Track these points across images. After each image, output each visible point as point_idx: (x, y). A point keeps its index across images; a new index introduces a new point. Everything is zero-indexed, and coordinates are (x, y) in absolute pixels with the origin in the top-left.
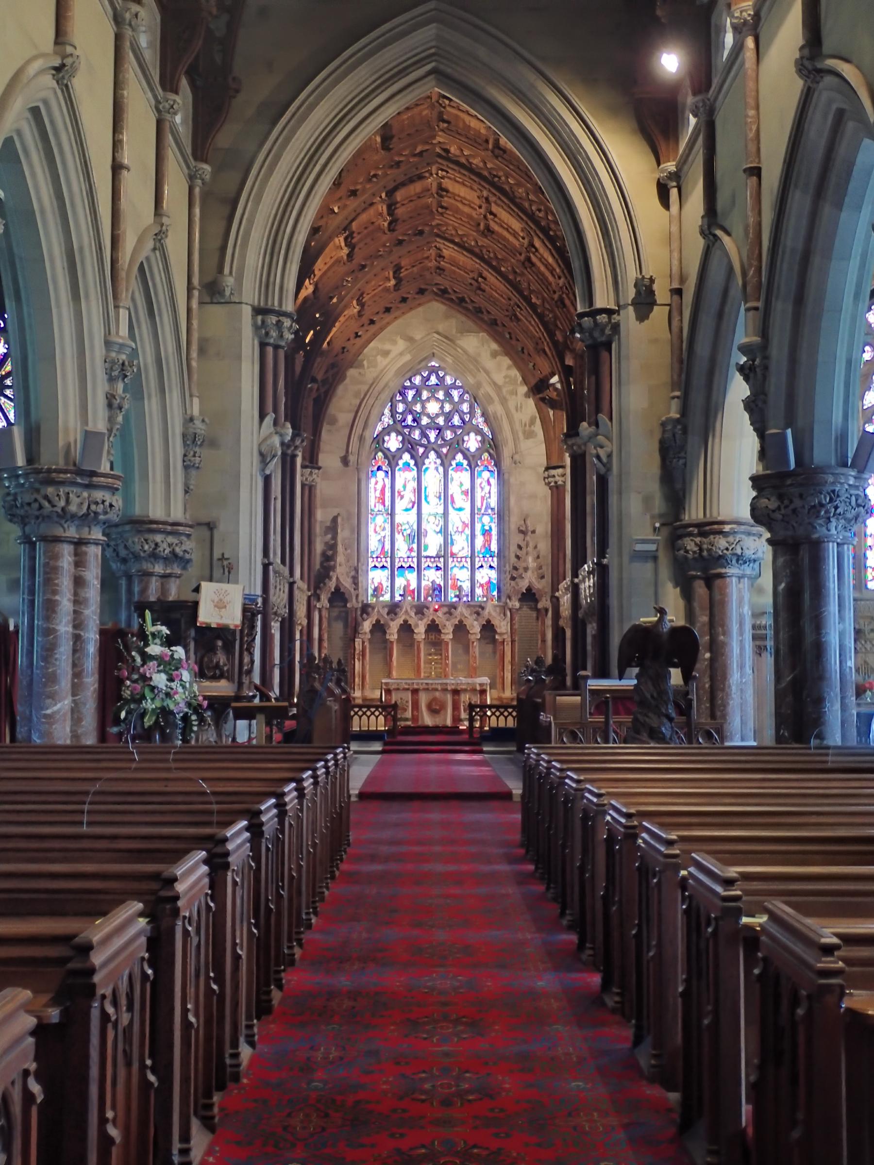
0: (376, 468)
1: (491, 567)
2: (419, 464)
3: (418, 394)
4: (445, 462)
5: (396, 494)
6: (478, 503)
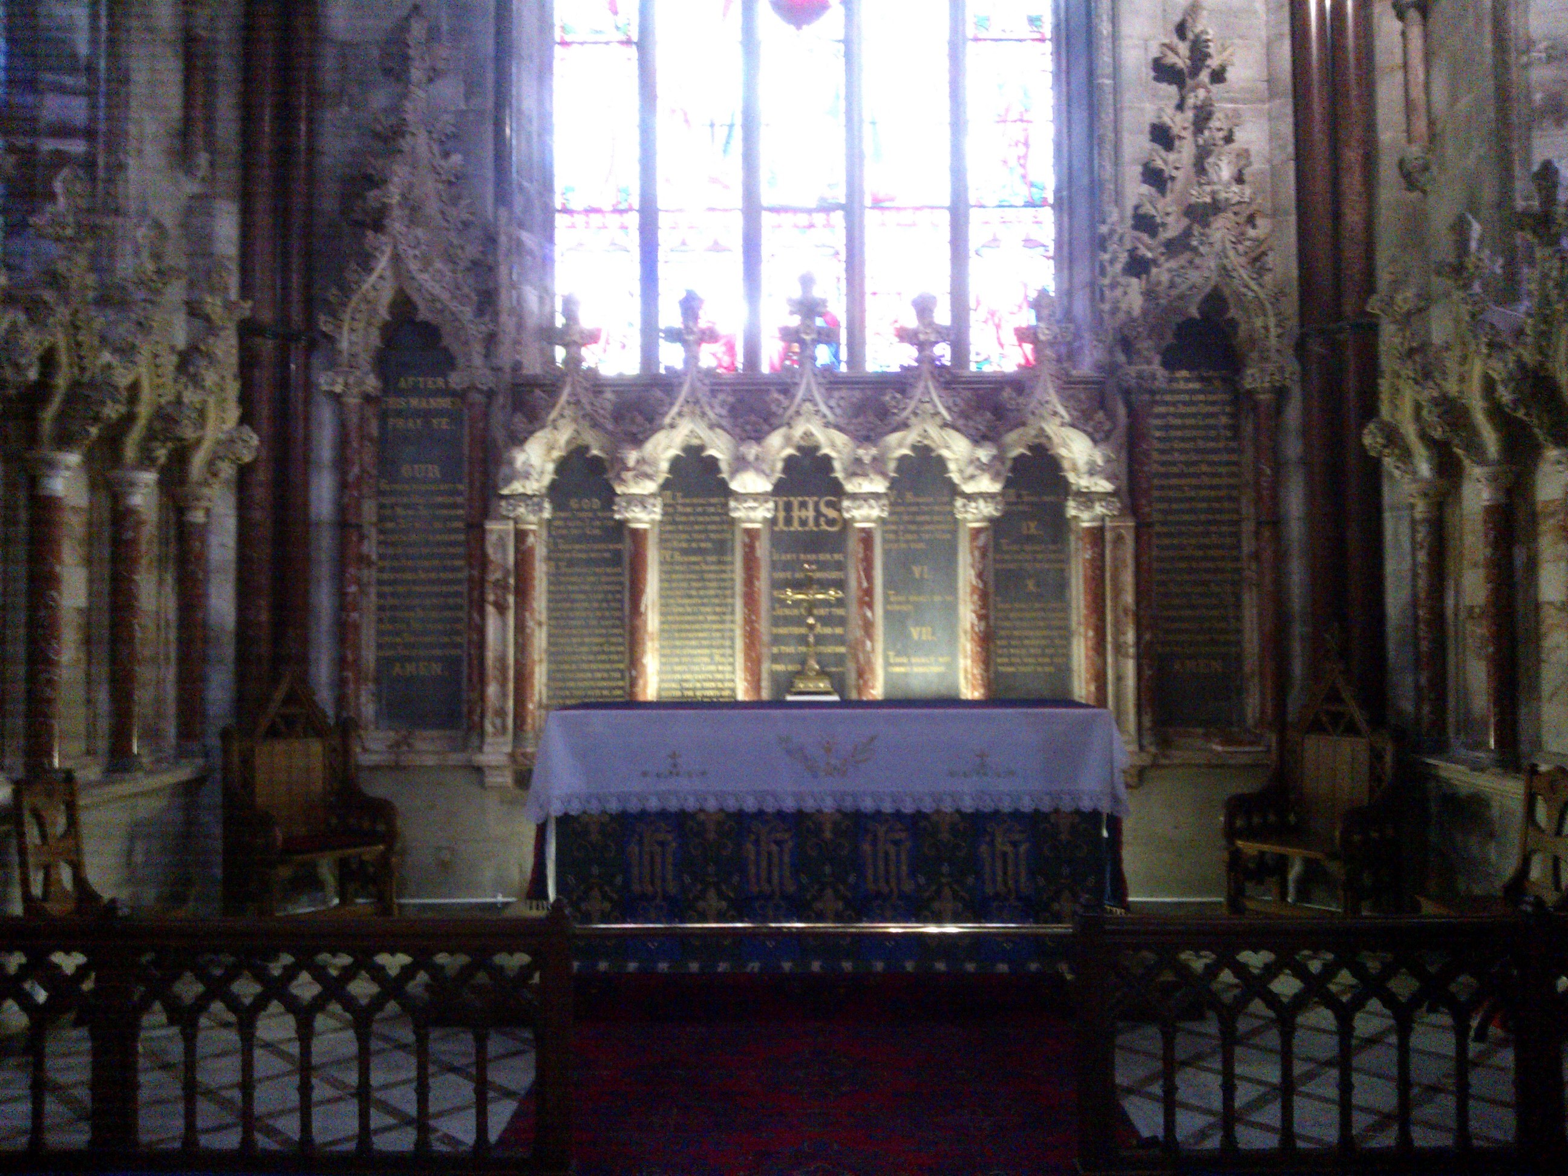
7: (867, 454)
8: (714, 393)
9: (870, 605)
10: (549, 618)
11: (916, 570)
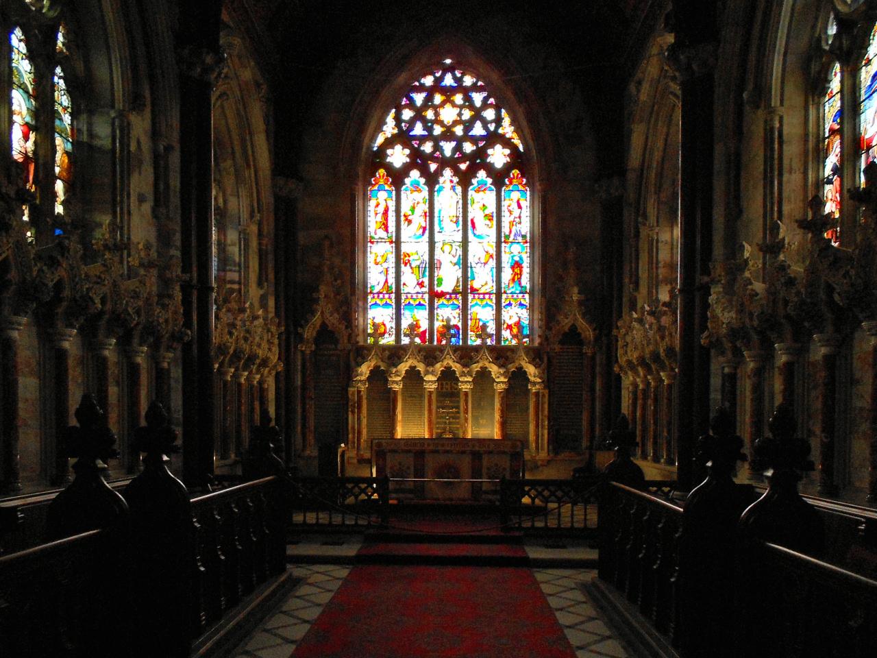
1: (521, 305)
2: (432, 180)
3: (429, 98)
4: (465, 180)
5: (403, 218)
6: (505, 230)
7: (466, 370)
8: (419, 352)
9: (467, 413)
10: (367, 415)
11: (482, 404)
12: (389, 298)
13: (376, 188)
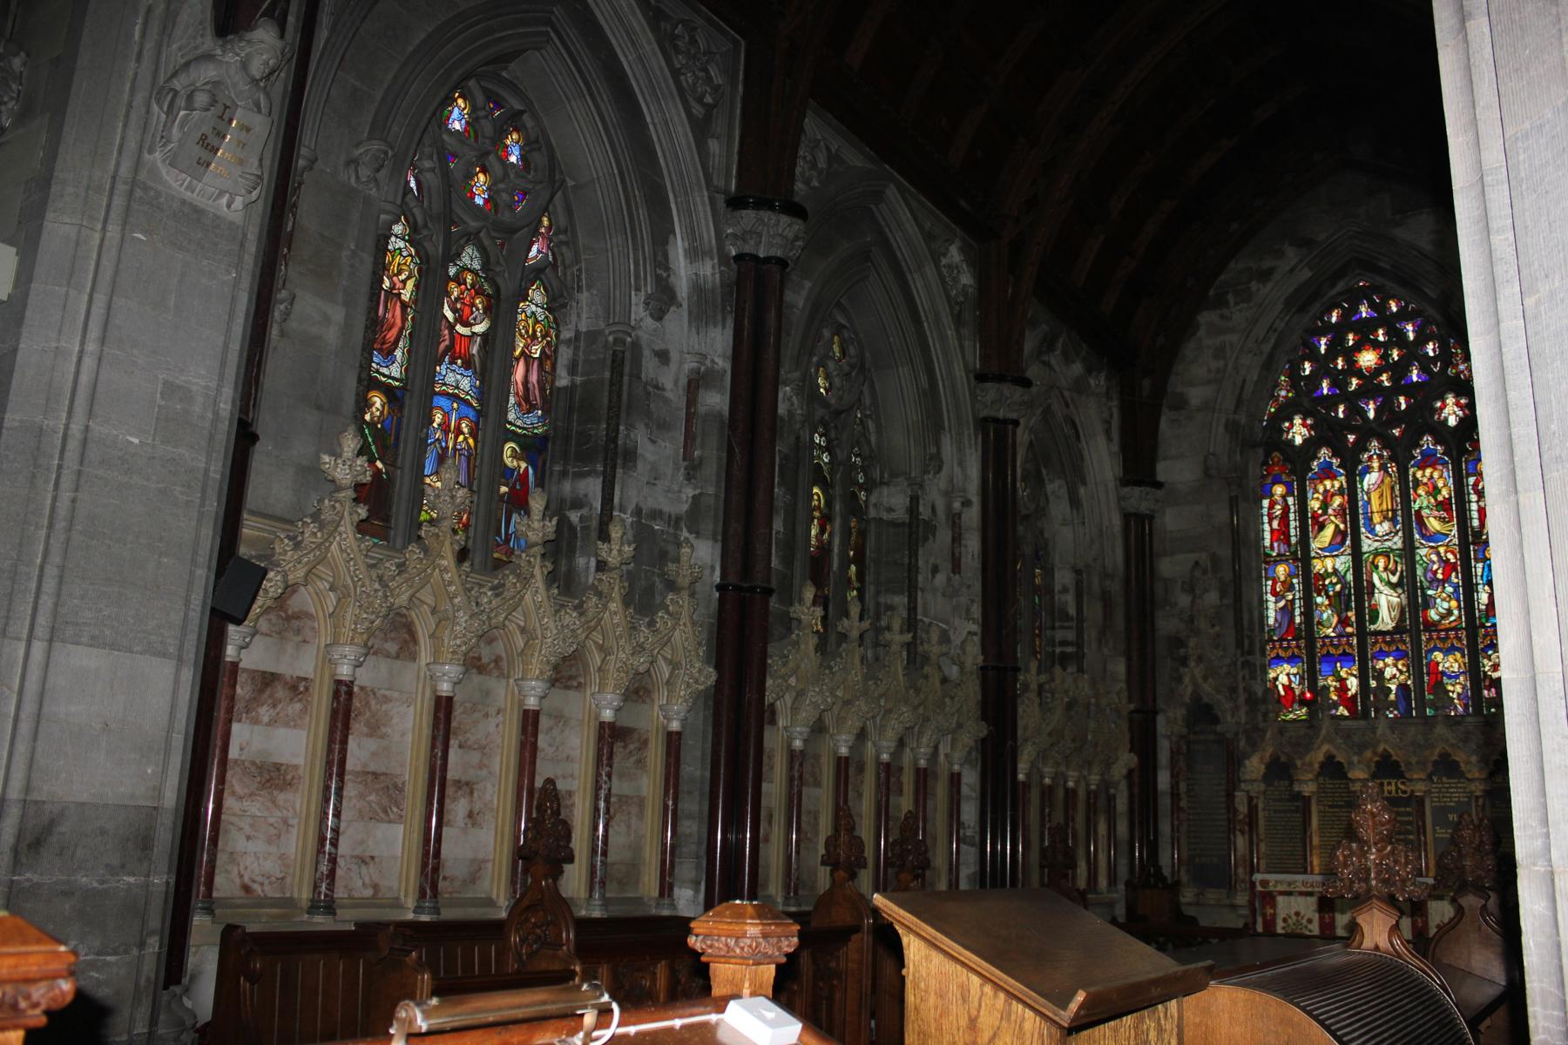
0: (1269, 480)
4: (1400, 456)
12: (1298, 647)
13: (1269, 480)
